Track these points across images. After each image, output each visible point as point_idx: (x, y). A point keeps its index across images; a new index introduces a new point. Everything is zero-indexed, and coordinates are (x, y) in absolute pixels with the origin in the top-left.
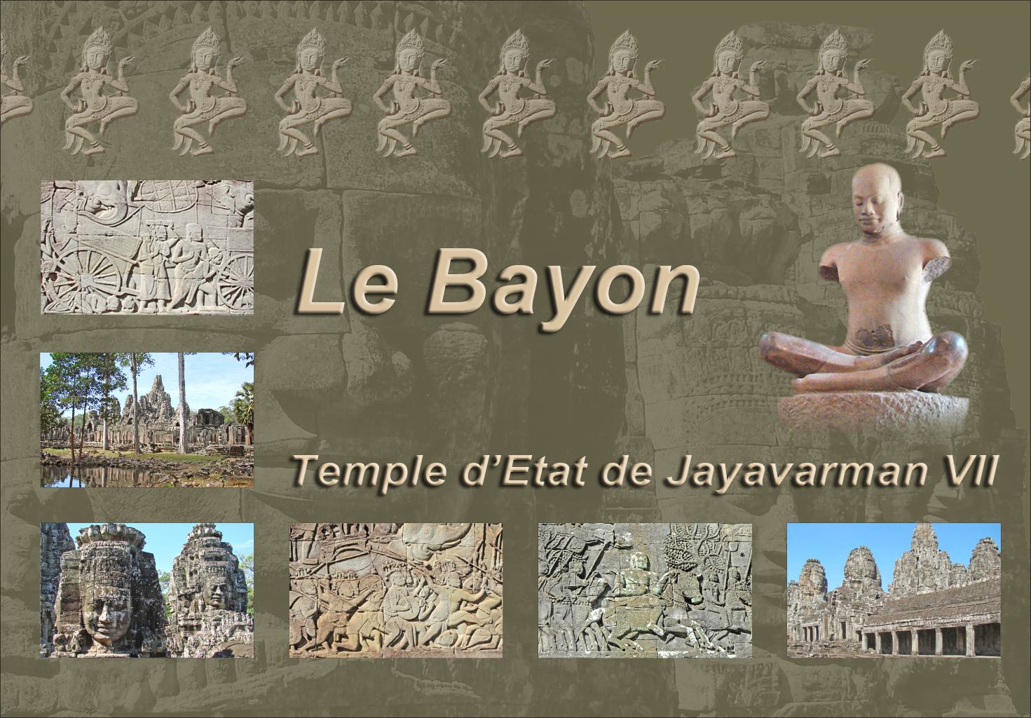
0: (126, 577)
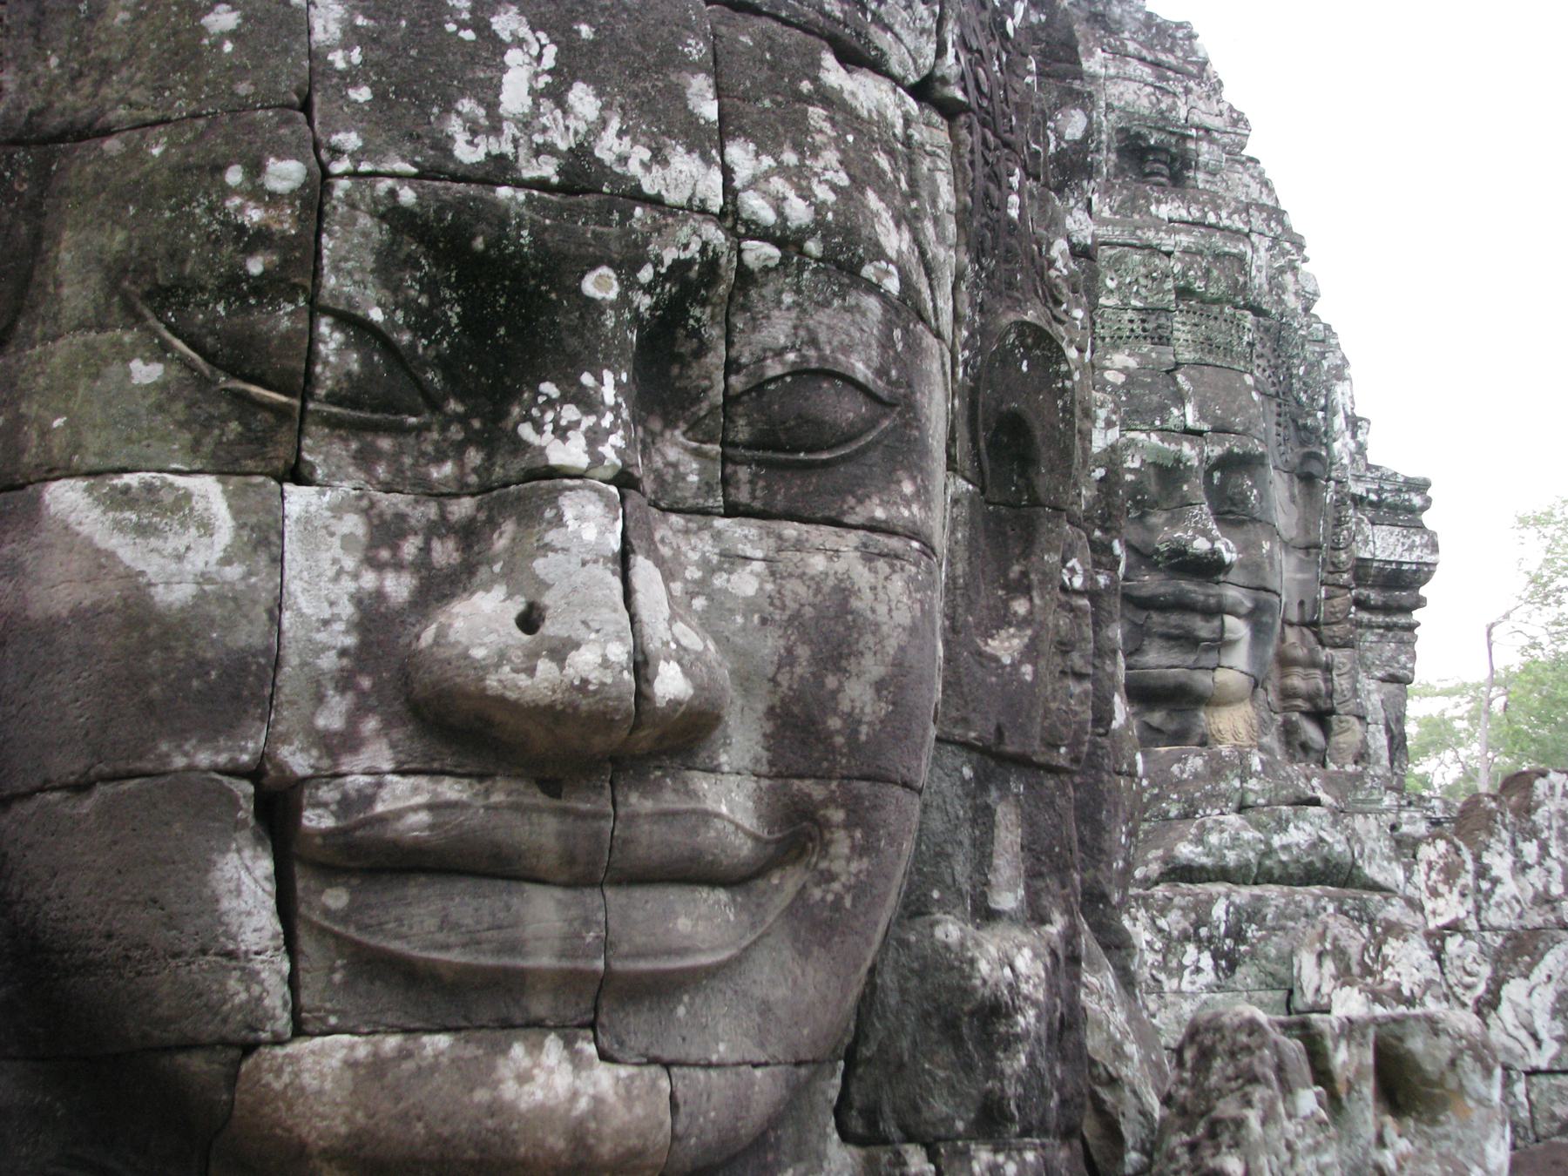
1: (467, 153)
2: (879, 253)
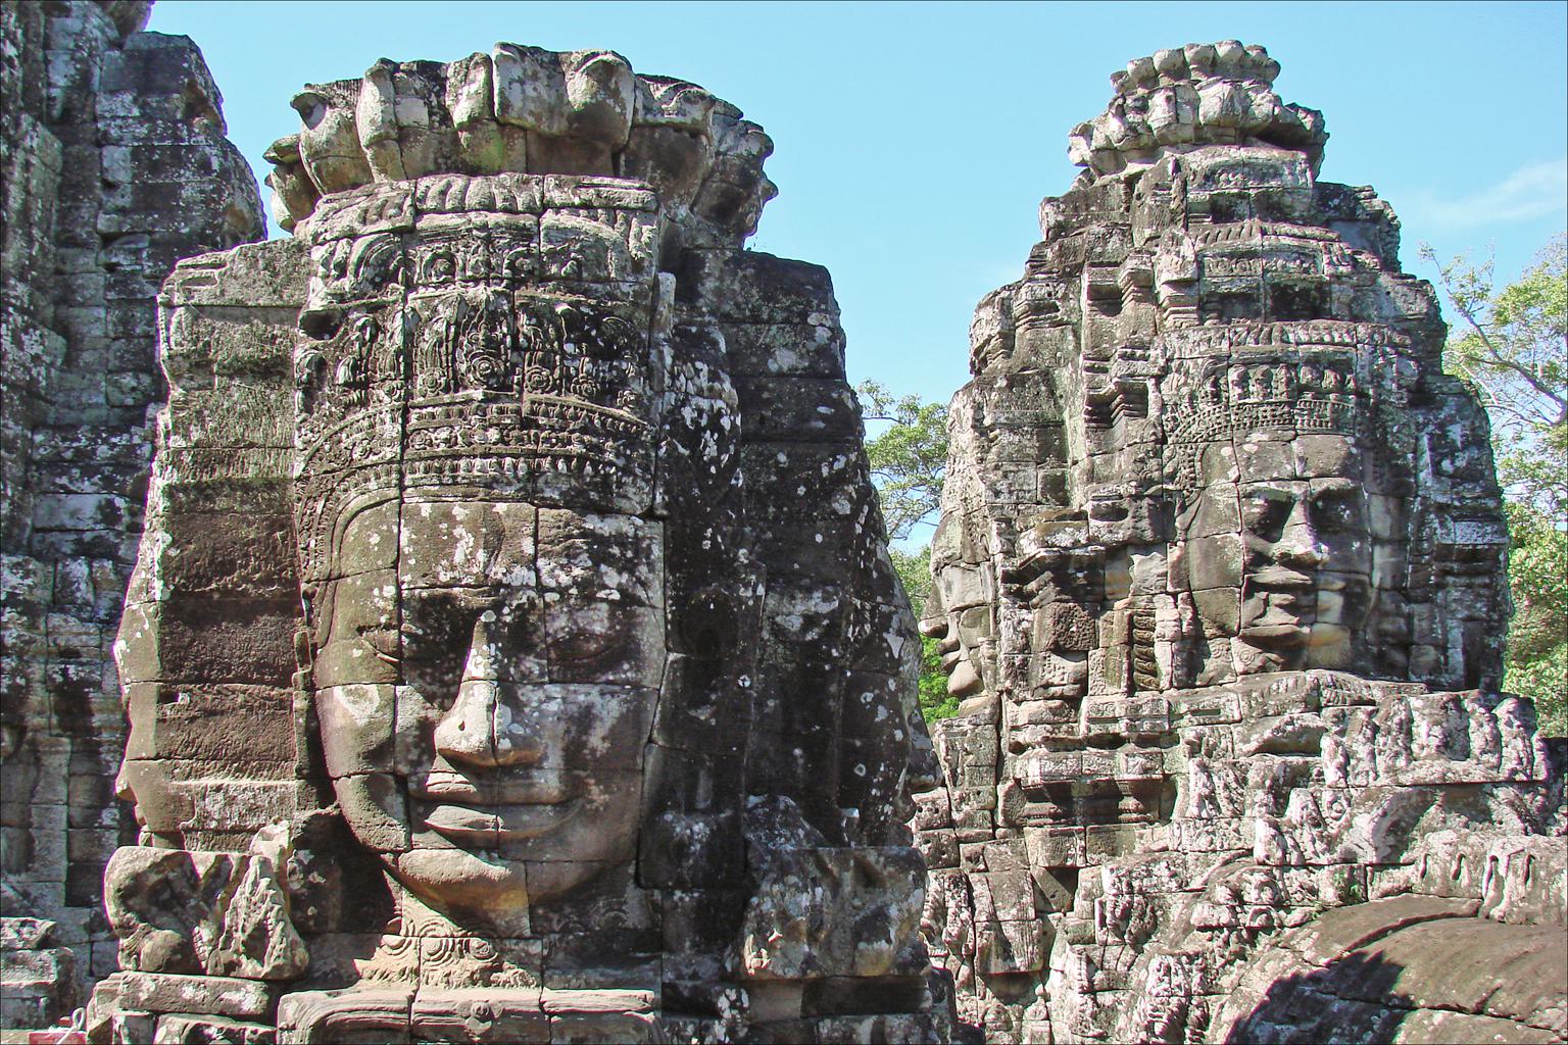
0: (629, 438)
1: (444, 578)
2: (605, 587)
